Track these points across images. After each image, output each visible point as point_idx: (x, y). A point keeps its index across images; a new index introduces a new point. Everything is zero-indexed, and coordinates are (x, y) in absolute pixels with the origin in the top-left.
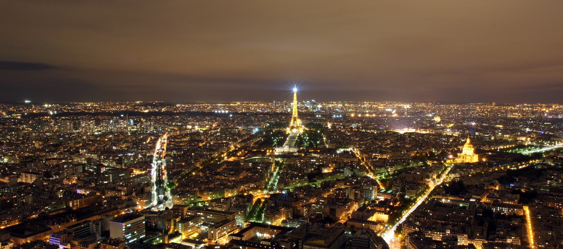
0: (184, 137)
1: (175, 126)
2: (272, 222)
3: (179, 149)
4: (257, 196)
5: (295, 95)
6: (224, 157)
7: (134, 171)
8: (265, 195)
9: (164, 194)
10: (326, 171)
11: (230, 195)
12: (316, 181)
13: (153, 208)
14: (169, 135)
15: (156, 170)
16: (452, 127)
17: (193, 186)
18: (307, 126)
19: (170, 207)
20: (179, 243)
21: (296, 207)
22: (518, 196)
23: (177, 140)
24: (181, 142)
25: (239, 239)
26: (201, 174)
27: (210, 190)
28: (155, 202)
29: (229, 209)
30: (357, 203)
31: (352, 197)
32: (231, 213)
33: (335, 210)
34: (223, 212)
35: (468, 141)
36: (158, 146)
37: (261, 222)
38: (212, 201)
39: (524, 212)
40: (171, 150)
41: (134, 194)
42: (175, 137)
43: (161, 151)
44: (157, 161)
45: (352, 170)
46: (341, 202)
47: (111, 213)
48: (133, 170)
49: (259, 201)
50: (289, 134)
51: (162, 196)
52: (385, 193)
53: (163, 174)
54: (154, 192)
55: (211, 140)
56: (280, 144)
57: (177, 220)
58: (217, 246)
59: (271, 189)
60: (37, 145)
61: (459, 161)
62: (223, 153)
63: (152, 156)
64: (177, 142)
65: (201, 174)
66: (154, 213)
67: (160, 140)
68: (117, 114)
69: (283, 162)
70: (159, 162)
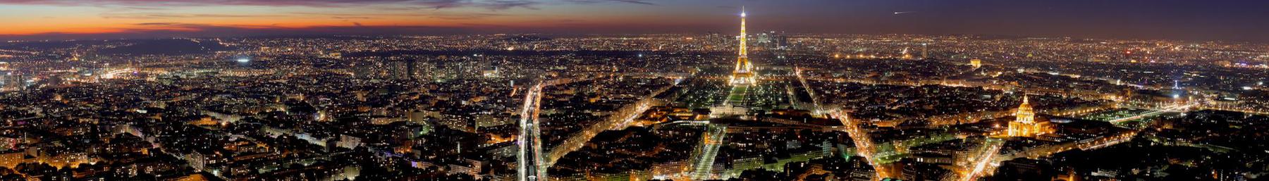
0: (567, 88)
1: (554, 71)
3: (559, 105)
5: (743, 23)
10: (789, 145)
16: (1000, 77)
18: (762, 73)
24: (564, 96)
26: (594, 146)
35: (1026, 100)
36: (528, 101)
40: (549, 107)
41: (492, 173)
42: (552, 89)
54: (522, 171)
56: (717, 102)
60: (360, 96)
61: (1011, 131)
63: (519, 117)
64: (557, 96)
65: (594, 146)
67: (530, 93)
68: (468, 53)
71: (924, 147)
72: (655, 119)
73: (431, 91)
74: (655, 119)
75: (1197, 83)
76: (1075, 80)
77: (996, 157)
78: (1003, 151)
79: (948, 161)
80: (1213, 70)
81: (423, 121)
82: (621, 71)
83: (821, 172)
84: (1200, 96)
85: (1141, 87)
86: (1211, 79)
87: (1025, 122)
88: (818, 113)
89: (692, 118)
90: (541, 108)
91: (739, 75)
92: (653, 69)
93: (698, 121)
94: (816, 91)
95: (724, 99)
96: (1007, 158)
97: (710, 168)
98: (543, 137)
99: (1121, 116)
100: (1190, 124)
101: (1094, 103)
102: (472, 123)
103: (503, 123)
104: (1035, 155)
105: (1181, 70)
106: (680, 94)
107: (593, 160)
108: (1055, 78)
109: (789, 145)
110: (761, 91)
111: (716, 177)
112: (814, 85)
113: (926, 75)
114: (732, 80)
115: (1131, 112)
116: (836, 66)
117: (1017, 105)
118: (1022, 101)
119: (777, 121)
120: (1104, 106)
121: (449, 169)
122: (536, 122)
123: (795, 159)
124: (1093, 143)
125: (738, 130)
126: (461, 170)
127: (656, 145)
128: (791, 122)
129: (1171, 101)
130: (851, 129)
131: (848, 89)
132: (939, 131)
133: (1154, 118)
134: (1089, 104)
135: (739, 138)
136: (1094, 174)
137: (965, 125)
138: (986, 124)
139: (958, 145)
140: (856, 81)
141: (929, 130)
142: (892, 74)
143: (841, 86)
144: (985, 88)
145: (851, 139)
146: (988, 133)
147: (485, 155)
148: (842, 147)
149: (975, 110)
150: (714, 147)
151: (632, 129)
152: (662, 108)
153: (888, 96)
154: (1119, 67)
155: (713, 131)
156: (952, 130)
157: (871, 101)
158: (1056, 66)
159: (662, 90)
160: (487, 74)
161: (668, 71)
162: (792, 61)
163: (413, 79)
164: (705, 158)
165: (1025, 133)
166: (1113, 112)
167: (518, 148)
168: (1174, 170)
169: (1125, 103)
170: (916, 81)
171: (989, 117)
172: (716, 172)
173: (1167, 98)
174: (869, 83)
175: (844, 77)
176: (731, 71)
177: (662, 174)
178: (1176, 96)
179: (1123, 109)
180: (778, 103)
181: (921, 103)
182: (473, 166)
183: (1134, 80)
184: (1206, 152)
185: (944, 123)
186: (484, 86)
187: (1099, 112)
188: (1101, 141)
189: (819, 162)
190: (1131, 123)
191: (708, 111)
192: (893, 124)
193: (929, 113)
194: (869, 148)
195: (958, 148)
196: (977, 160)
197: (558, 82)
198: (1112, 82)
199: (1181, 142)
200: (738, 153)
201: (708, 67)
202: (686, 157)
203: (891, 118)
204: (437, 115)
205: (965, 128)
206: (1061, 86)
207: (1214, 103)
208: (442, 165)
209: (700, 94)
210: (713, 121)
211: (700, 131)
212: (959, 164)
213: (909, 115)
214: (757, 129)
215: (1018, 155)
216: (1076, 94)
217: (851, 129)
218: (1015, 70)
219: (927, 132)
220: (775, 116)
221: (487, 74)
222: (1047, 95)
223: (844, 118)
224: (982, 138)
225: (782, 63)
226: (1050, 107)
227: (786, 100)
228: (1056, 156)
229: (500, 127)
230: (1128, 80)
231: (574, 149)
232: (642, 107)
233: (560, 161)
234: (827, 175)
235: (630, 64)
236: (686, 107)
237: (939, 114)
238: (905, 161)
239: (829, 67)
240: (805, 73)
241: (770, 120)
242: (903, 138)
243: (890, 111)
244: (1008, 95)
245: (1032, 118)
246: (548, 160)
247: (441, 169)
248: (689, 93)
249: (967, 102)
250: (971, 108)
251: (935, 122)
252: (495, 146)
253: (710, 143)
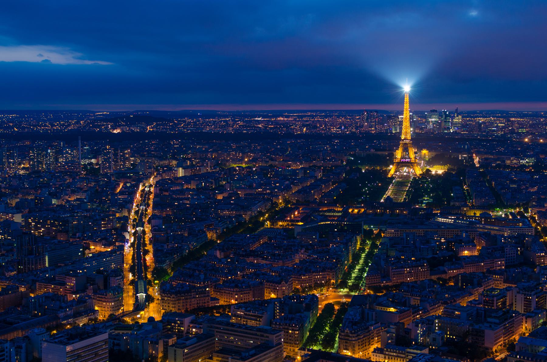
4: (327, 298)
6: (264, 221)
7: (92, 247)
8: (341, 297)
9: (146, 291)
15: (132, 245)
17: (202, 277)
21: (403, 324)
24: (182, 192)
30: (530, 321)
31: (519, 307)
33: (483, 332)
34: (259, 330)
37: (333, 351)
44: (134, 227)
46: (495, 317)
49: (329, 307)
50: (392, 178)
51: (142, 296)
53: (146, 252)
57: (171, 342)
59: (355, 287)
62: (262, 214)
66: (128, 327)
69: (379, 235)
91: (401, 164)
176: (390, 160)
252: (100, 254)
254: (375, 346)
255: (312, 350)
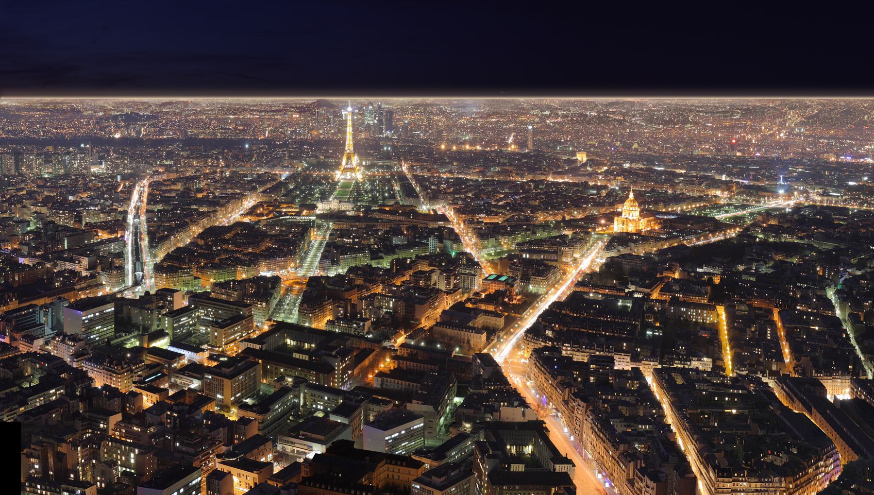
0: (174, 183)
1: (161, 165)
2: (310, 323)
3: (165, 200)
10: (396, 241)
11: (244, 276)
12: (382, 258)
13: (126, 292)
14: (151, 180)
16: (606, 171)
18: (368, 168)
19: (153, 292)
20: (165, 347)
22: (709, 288)
23: (163, 188)
24: (171, 191)
25: (258, 347)
26: (201, 242)
27: (215, 266)
28: (130, 281)
29: (243, 299)
32: (247, 306)
36: (135, 197)
38: (216, 285)
39: (718, 315)
41: (99, 269)
43: (139, 204)
45: (441, 242)
47: (65, 296)
48: (97, 232)
50: (339, 182)
52: (496, 279)
54: (129, 267)
55: (216, 189)
56: (324, 197)
58: (224, 356)
61: (617, 227)
63: (125, 213)
65: (201, 242)
67: (137, 188)
70: (137, 220)
71: (530, 243)
72: (262, 215)
73: (38, 186)
74: (262, 215)
75: (801, 178)
76: (681, 175)
77: (602, 253)
78: (608, 247)
79: (553, 257)
80: (818, 165)
81: (31, 216)
82: (227, 166)
83: (427, 268)
84: (805, 192)
85: (746, 182)
86: (817, 174)
87: (630, 218)
88: (424, 208)
89: (298, 214)
90: (148, 203)
91: (346, 170)
92: (259, 163)
93: (305, 216)
94: (422, 186)
95: (330, 194)
96: (613, 254)
97: (316, 264)
98: (149, 233)
99: (727, 212)
100: (797, 220)
101: (700, 199)
102: (79, 219)
103: (110, 218)
104: (641, 251)
105: (786, 164)
106: (287, 188)
107: (201, 255)
108: (661, 173)
109: (396, 241)
110: (368, 186)
111: (323, 274)
112: (419, 180)
113: (532, 170)
114: (338, 175)
115: (736, 207)
116: (442, 159)
117: (622, 201)
118: (627, 197)
119: (384, 216)
120: (709, 201)
121: (56, 265)
122: (143, 218)
123: (401, 255)
124: (698, 239)
125: (344, 226)
126: (68, 266)
127: (262, 240)
128: (398, 218)
129: (775, 195)
130: (457, 224)
131: (454, 184)
132: (545, 226)
133: (759, 213)
134: (694, 200)
135: (344, 233)
136: (699, 270)
137: (570, 220)
138: (591, 220)
139: (564, 241)
140: (462, 176)
141: (534, 225)
142: (498, 169)
143: (447, 181)
144: (591, 184)
145: (457, 235)
146: (594, 229)
147: (90, 250)
148: (448, 243)
149: (583, 205)
150: (321, 244)
151: (238, 224)
152: (269, 204)
153: (495, 191)
154: (724, 162)
155: (319, 227)
156: (557, 226)
157: (476, 197)
158: (661, 162)
159: (269, 186)
160: (94, 169)
161: (274, 166)
162: (398, 154)
163: (20, 174)
164: (312, 253)
165: (631, 229)
166: (719, 208)
167: (125, 244)
168: (779, 265)
169: (730, 199)
170: (522, 176)
171: (595, 212)
172: (322, 268)
173: (771, 192)
174: (475, 178)
175: (450, 172)
176: (337, 165)
177: (269, 270)
178: (781, 192)
179: (729, 205)
180: (384, 198)
181: (527, 198)
182: (80, 262)
183: (739, 175)
184: (811, 248)
185: (550, 218)
186: (91, 181)
187: (705, 207)
188: (706, 237)
189: (425, 258)
190: (736, 219)
191: (314, 207)
192: (499, 220)
193: (535, 209)
194: (475, 244)
195: (564, 244)
196: (583, 256)
197: (165, 177)
198: (717, 177)
199: (787, 238)
200: (344, 250)
201: (315, 161)
202: (292, 253)
203: (497, 214)
204: (44, 210)
205: (569, 224)
206: (667, 181)
207: (819, 198)
208: (49, 261)
209: (307, 188)
210: (320, 216)
211: (306, 228)
212: (564, 260)
213: (515, 211)
214: (363, 225)
215: (624, 251)
216: (682, 189)
217: (457, 224)
218: (620, 165)
219: (533, 228)
220: (381, 211)
221: (94, 169)
222: (653, 190)
223: (450, 213)
224: (588, 233)
225: (387, 156)
226: (656, 203)
227: (393, 197)
228: (661, 252)
229: (106, 222)
230: (734, 175)
231: (181, 245)
232: (249, 202)
233: (168, 257)
234: (432, 271)
235: (236, 157)
236: (292, 202)
237: (545, 210)
238: (511, 257)
239: (435, 161)
240: (411, 168)
241: (376, 215)
242: (509, 234)
243: (496, 206)
244: (614, 189)
245: (638, 213)
246: (155, 256)
247: (48, 265)
248: (296, 188)
249: (574, 196)
250: (577, 204)
251: (541, 217)
252: (103, 242)
253: (317, 238)
254: (328, 318)
255: (277, 321)
